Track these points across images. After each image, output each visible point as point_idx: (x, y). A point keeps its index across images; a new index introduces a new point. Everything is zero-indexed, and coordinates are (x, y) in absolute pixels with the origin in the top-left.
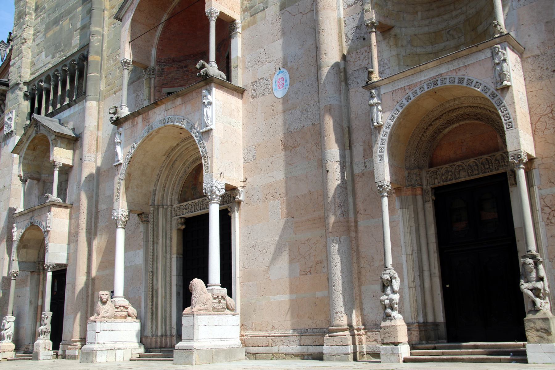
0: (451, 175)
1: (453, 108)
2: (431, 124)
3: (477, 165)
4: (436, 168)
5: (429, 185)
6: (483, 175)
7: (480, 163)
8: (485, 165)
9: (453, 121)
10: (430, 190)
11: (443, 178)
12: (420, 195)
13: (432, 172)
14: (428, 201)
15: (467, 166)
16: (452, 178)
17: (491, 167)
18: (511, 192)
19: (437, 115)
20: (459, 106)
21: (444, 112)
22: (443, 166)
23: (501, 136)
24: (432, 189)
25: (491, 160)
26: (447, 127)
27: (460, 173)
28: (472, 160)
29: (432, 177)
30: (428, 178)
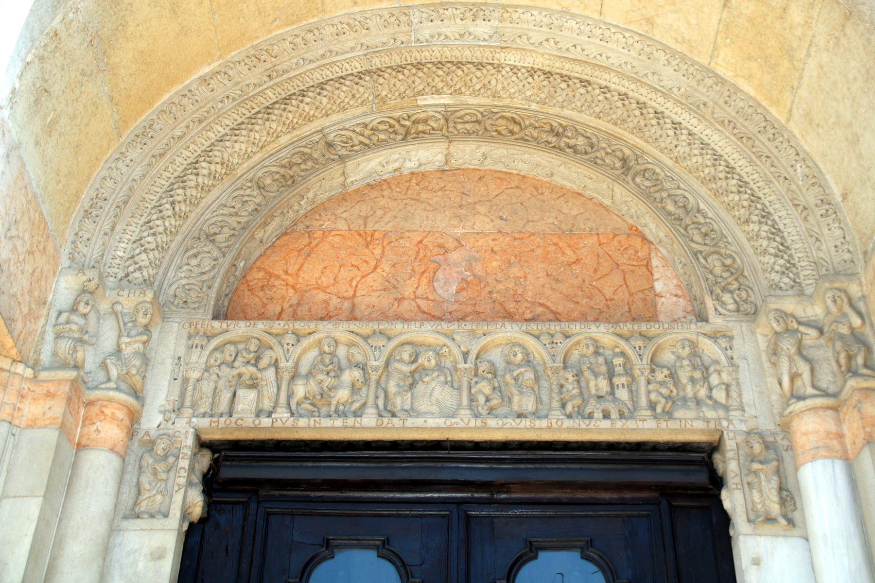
0: (354, 389)
1: (448, 54)
2: (303, 94)
3: (528, 362)
4: (261, 325)
5: (188, 412)
6: (568, 423)
7: (560, 358)
8: (587, 374)
9: (421, 127)
10: (190, 441)
11: (300, 390)
12: (112, 450)
13: (230, 342)
14: (152, 516)
15: (472, 356)
16: (356, 406)
17: (623, 394)
18: (757, 562)
19: (348, 61)
20: (486, 56)
21: (397, 60)
22: (312, 326)
23: (689, 247)
24: (203, 445)
25: (623, 354)
26: (381, 145)
27: (420, 388)
28: (510, 332)
29: (226, 370)
30: (195, 375)
